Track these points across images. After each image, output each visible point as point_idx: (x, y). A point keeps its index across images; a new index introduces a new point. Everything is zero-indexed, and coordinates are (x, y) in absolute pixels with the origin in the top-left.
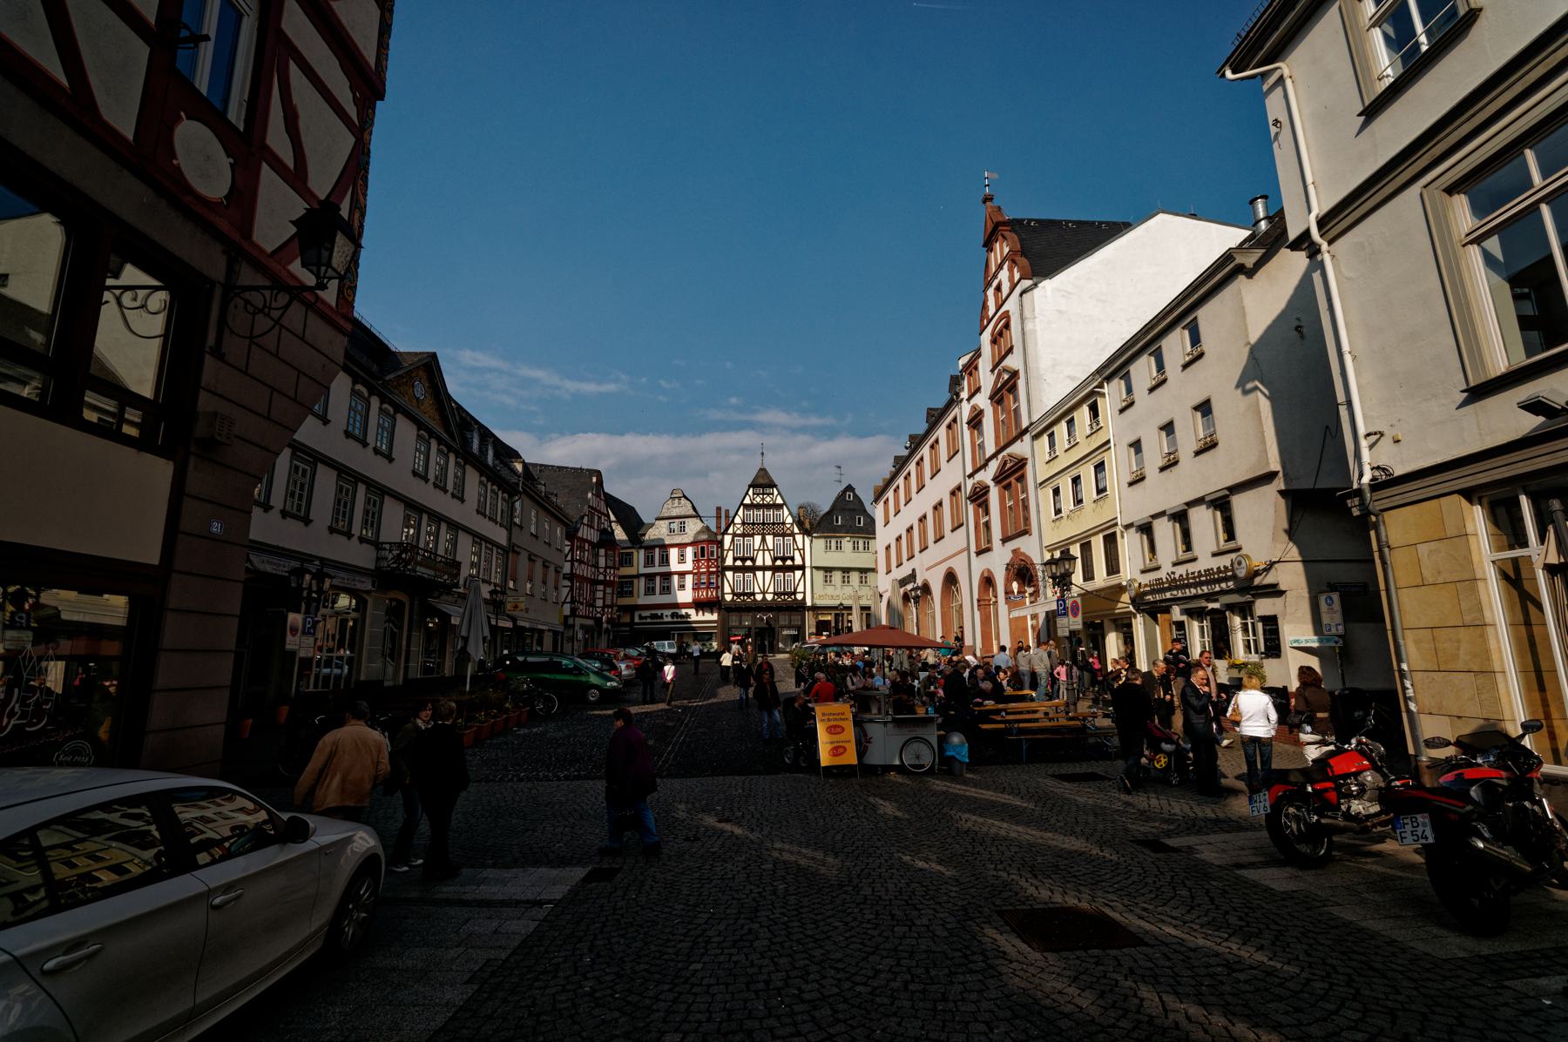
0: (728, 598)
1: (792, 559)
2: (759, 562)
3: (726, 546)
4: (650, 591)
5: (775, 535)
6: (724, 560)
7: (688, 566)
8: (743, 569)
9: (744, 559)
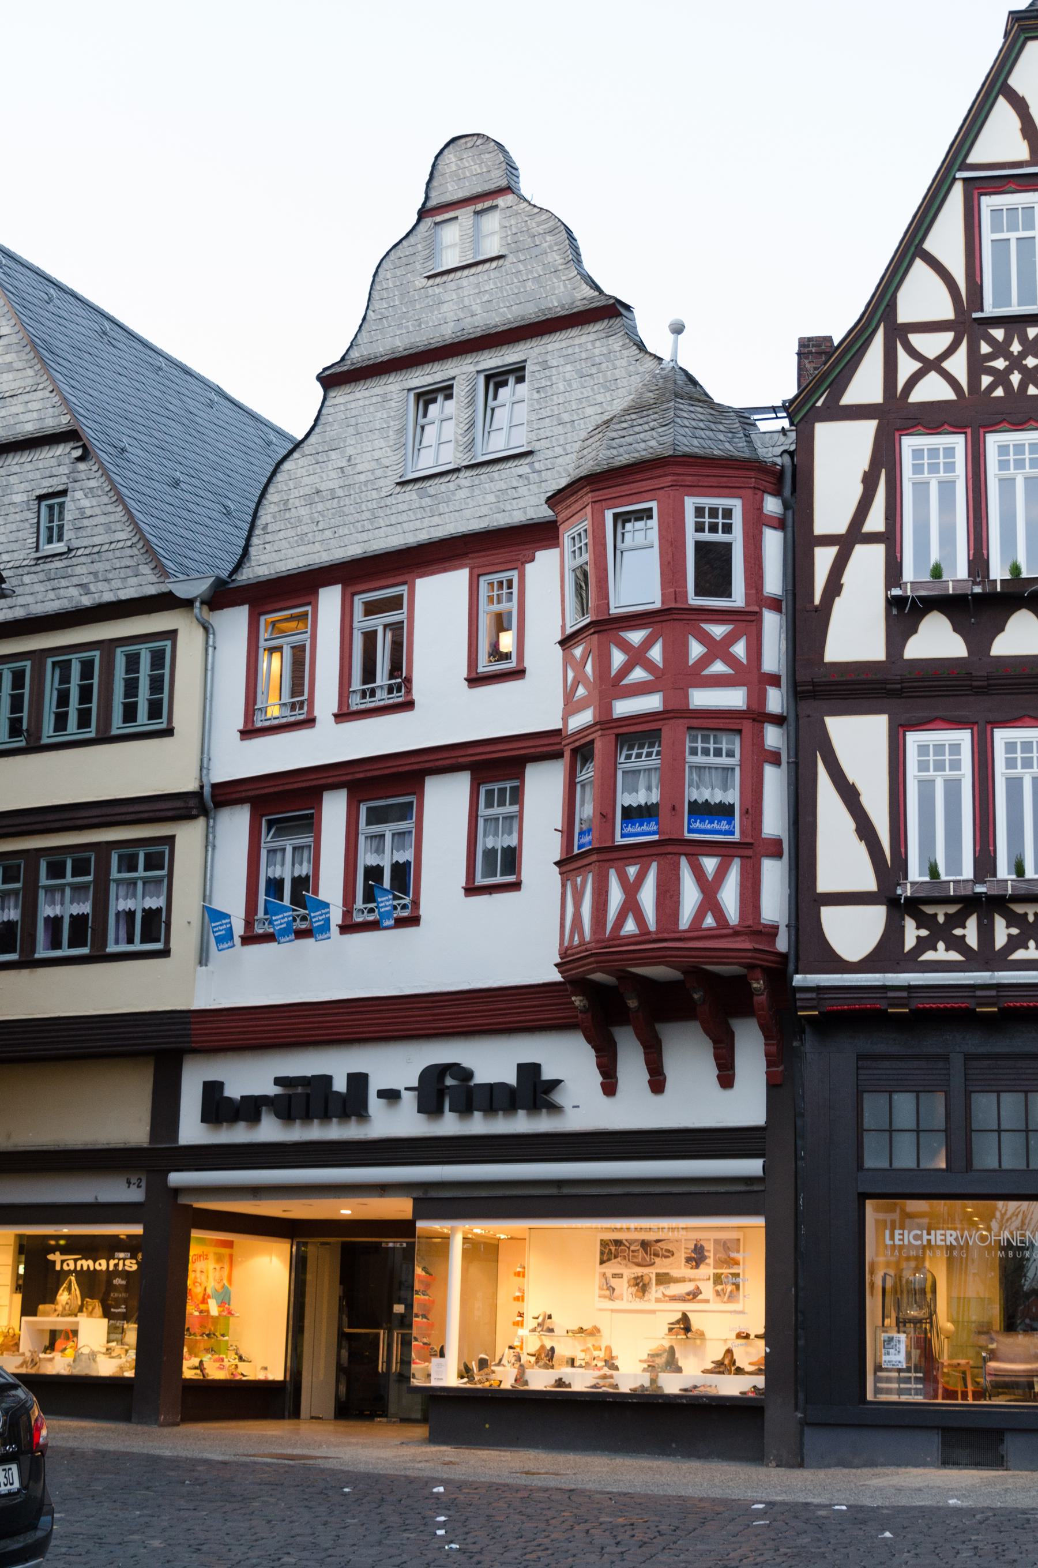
3: (832, 508)
4: (284, 909)
6: (808, 620)
7: (535, 703)
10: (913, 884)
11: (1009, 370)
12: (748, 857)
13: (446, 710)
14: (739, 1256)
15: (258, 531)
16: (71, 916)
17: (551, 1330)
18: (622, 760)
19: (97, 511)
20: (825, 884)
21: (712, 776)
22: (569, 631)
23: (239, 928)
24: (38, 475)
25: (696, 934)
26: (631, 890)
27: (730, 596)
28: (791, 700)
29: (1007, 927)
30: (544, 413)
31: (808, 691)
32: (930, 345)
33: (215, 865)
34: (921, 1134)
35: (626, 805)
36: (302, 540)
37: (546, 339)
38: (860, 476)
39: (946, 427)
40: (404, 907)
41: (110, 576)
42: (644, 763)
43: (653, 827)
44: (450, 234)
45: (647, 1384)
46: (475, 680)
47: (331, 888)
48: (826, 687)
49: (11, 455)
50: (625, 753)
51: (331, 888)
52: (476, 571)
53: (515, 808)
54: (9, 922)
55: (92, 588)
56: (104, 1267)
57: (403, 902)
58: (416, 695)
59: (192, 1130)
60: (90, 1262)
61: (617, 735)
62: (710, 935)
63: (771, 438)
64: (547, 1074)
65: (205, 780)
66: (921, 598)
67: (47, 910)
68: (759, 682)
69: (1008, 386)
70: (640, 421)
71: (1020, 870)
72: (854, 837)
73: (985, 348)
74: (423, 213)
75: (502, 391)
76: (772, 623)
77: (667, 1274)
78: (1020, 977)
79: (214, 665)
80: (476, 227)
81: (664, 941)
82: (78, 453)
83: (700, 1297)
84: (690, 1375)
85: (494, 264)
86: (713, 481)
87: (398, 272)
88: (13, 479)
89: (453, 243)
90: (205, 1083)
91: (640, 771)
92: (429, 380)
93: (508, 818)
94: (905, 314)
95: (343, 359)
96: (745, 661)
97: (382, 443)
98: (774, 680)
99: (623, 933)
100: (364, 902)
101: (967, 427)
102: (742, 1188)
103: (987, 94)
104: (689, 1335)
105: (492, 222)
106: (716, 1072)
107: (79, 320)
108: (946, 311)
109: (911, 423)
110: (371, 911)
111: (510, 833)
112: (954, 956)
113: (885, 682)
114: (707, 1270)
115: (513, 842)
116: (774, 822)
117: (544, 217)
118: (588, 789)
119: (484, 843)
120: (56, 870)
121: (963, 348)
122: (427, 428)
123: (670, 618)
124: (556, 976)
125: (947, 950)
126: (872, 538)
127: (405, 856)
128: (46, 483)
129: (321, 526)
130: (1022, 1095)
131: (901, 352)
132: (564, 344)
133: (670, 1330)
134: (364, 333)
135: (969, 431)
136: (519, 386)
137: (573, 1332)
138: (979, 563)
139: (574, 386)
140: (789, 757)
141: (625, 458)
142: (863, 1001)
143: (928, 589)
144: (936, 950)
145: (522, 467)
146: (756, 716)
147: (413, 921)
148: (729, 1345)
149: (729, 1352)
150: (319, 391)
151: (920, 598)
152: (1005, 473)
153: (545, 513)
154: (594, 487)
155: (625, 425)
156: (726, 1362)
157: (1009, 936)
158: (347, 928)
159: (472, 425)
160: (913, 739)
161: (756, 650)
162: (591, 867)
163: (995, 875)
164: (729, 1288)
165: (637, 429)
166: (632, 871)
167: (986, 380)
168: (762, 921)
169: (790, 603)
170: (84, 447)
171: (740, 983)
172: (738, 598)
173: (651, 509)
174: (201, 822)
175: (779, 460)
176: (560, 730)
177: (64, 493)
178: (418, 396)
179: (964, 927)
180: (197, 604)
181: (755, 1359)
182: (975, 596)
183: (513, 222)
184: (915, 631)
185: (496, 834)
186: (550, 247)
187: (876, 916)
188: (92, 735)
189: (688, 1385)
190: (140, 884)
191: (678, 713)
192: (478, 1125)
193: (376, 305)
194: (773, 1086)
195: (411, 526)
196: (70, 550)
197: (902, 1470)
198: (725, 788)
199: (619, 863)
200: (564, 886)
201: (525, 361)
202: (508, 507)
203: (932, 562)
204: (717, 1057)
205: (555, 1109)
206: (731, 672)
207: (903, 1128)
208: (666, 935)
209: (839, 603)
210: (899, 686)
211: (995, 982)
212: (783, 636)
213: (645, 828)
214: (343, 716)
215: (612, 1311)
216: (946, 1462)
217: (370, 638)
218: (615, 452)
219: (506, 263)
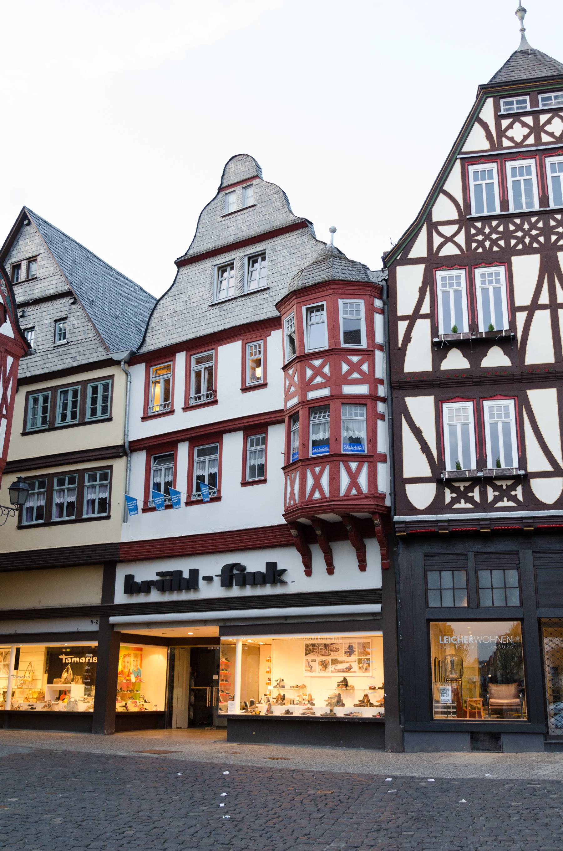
0: (421, 496)
3: (405, 304)
4: (161, 496)
6: (395, 353)
8: (475, 386)
9: (474, 346)
10: (449, 472)
11: (484, 240)
13: (234, 403)
15: (149, 331)
16: (68, 502)
17: (283, 687)
18: (312, 419)
19: (80, 325)
20: (407, 474)
22: (286, 363)
23: (141, 505)
24: (55, 311)
25: (348, 498)
28: (389, 391)
29: (493, 492)
30: (274, 271)
31: (397, 386)
32: (448, 231)
33: (131, 477)
34: (455, 590)
36: (168, 333)
37: (274, 239)
39: (456, 266)
40: (214, 493)
41: (85, 353)
42: (322, 420)
43: (327, 449)
44: (232, 198)
45: (328, 712)
46: (245, 389)
47: (181, 486)
48: (406, 385)
49: (44, 304)
50: (313, 416)
51: (181, 486)
52: (245, 341)
53: (264, 446)
54: (40, 506)
55: (78, 358)
56: (84, 661)
57: (213, 491)
58: (219, 398)
59: (120, 597)
60: (78, 659)
61: (310, 408)
62: (354, 498)
64: (280, 567)
65: (126, 440)
67: (57, 500)
68: (375, 382)
69: (484, 247)
70: (317, 267)
71: (498, 465)
73: (473, 231)
74: (220, 189)
75: (255, 265)
76: (379, 356)
77: (336, 659)
78: (500, 515)
79: (130, 390)
80: (243, 194)
82: (72, 301)
83: (352, 670)
84: (348, 708)
85: (251, 209)
86: (351, 292)
87: (210, 216)
88: (44, 314)
89: (233, 201)
90: (126, 576)
92: (224, 260)
93: (261, 451)
94: (436, 218)
95: (186, 254)
96: (367, 373)
97: (203, 289)
98: (381, 382)
99: (313, 498)
100: (197, 491)
101: (466, 266)
102: (371, 618)
103: (470, 121)
104: (347, 688)
105: (250, 192)
106: (358, 564)
107: (76, 251)
108: (455, 216)
109: (440, 265)
110: (199, 495)
111: (262, 458)
112: (469, 506)
113: (432, 380)
115: (263, 462)
116: (383, 446)
117: (273, 187)
118: (296, 434)
119: (250, 463)
120: (61, 482)
121: (463, 231)
122: (223, 282)
123: (333, 353)
124: (283, 521)
125: (465, 503)
126: (424, 316)
127: (214, 470)
128: (58, 314)
129: (177, 327)
130: (502, 571)
131: (435, 235)
132: (282, 241)
133: (338, 685)
134: (195, 242)
135: (467, 268)
136: (263, 262)
137: (294, 687)
138: (474, 325)
139: (287, 259)
140: (389, 416)
141: (310, 282)
142: (427, 528)
143: (451, 337)
144: (460, 503)
145: (265, 295)
146: (373, 398)
147: (218, 499)
148: (366, 692)
149: (366, 696)
150: (175, 268)
152: (484, 286)
153: (276, 313)
155: (310, 269)
156: (365, 701)
157: (494, 496)
158: (188, 504)
159: (242, 278)
161: (372, 368)
162: (298, 469)
163: (486, 467)
164: (365, 665)
165: (316, 271)
166: (317, 469)
167: (474, 245)
168: (379, 492)
169: (387, 346)
170: (75, 298)
171: (369, 521)
172: (364, 344)
173: (323, 305)
174: (124, 458)
176: (283, 410)
177: (66, 318)
178: (219, 268)
179: (473, 492)
180: (123, 363)
181: (379, 699)
182: (472, 339)
183: (259, 190)
184: (445, 357)
185: (255, 459)
186: (276, 200)
187: (432, 488)
188: (77, 422)
189: (348, 712)
190: (97, 487)
192: (249, 592)
193: (200, 230)
194: (385, 570)
195: (216, 324)
196: (68, 343)
197: (453, 754)
198: (360, 432)
199: (311, 466)
200: (286, 479)
201: (265, 249)
202: (259, 313)
204: (358, 557)
205: (283, 583)
206: (361, 377)
207: (446, 586)
208: (334, 499)
209: (410, 346)
210: (439, 382)
212: (385, 362)
213: (323, 450)
214: (187, 408)
215: (311, 677)
216: (473, 749)
217: (198, 375)
218: (306, 281)
219: (256, 208)
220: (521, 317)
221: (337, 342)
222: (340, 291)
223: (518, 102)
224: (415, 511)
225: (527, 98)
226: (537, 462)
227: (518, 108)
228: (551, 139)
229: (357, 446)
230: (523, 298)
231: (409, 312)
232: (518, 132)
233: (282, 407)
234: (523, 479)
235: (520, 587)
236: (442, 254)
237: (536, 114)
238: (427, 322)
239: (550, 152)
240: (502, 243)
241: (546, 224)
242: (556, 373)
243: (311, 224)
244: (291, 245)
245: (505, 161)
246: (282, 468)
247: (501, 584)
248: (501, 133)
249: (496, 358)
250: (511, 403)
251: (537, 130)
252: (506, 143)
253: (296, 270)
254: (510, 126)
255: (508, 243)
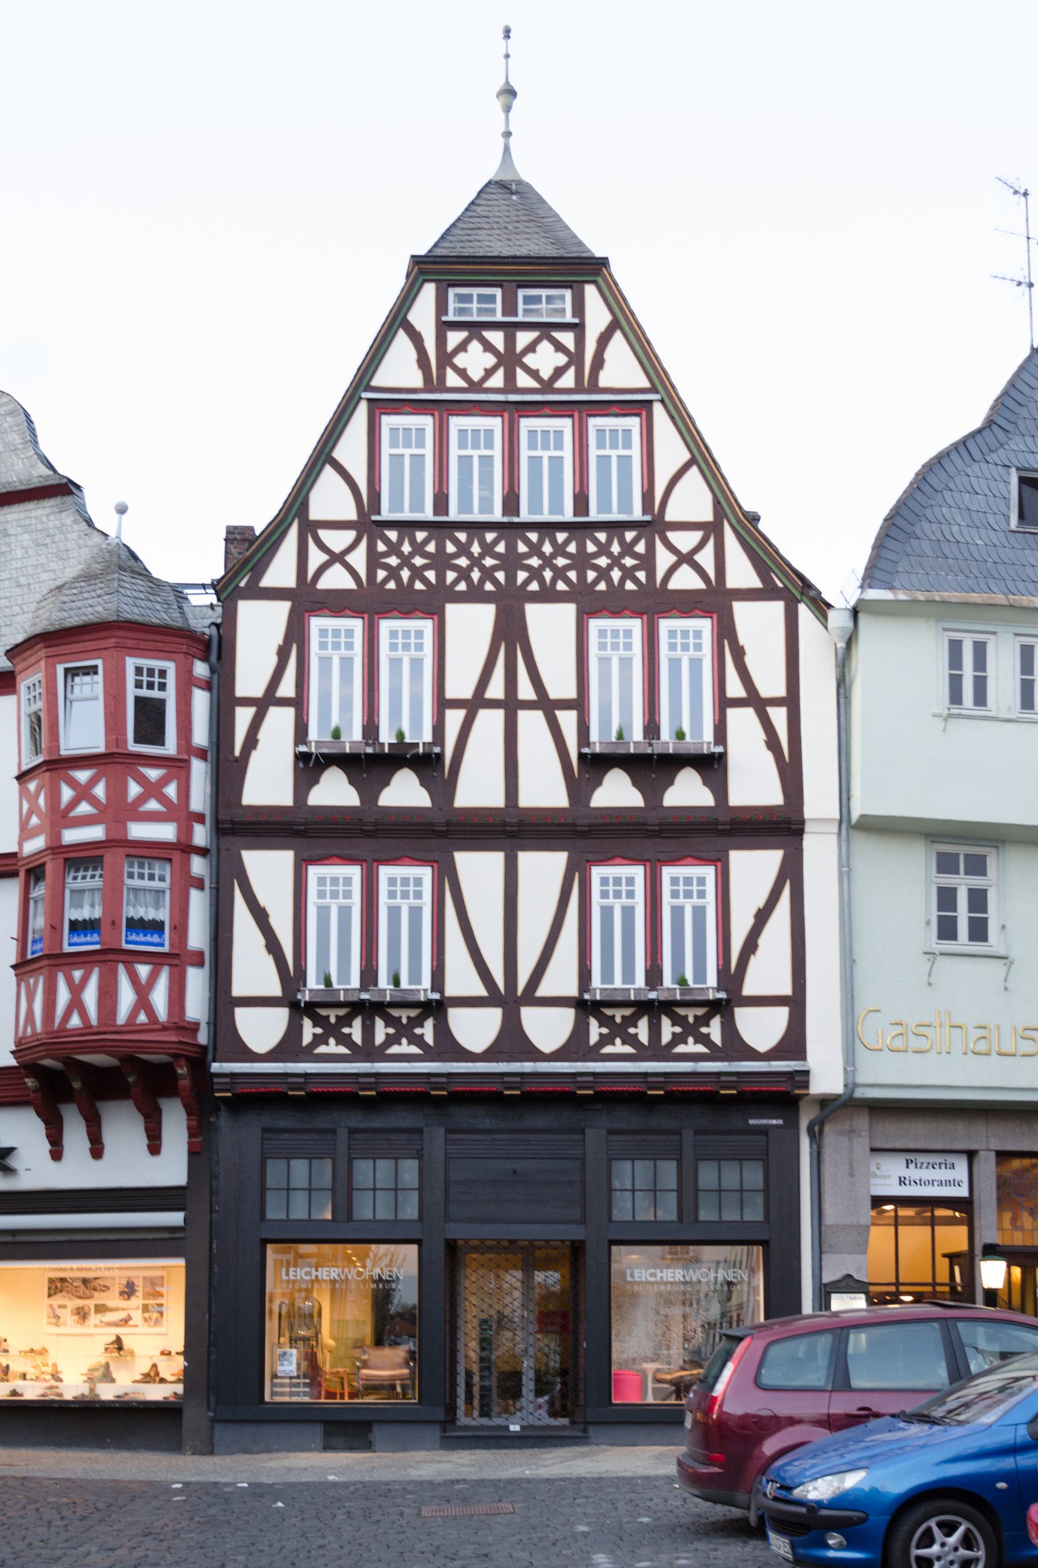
0: (261, 1029)
1: (711, 766)
2: (478, 788)
3: (251, 677)
5: (591, 604)
6: (229, 769)
8: (367, 838)
9: (370, 766)
10: (311, 991)
12: (177, 966)
14: (163, 1290)
17: (6, 1351)
20: (238, 990)
21: (147, 895)
22: (25, 768)
26: (76, 990)
27: (163, 744)
35: (73, 919)
38: (275, 649)
42: (89, 883)
43: (96, 938)
45: (86, 1392)
48: (244, 826)
61: (66, 859)
62: (142, 1030)
63: (201, 611)
66: (323, 755)
68: (187, 819)
71: (396, 981)
72: (264, 951)
73: (381, 547)
76: (199, 770)
77: (104, 1305)
81: (103, 1033)
83: (131, 1323)
84: (123, 1385)
91: (84, 891)
96: (175, 801)
98: (200, 818)
101: (364, 612)
102: (167, 1235)
104: (122, 1353)
113: (292, 823)
114: (137, 1301)
116: (198, 937)
126: (284, 702)
130: (393, 1162)
133: (106, 1349)
135: (366, 616)
137: (25, 1352)
138: (371, 729)
146: (185, 848)
148: (155, 1360)
149: (155, 1366)
151: (322, 755)
152: (394, 654)
154: (47, 643)
155: (75, 591)
156: (152, 1374)
160: (314, 872)
161: (184, 792)
162: (42, 971)
163: (376, 985)
164: (155, 1315)
166: (77, 974)
167: (381, 574)
168: (187, 1019)
171: (167, 1069)
172: (170, 747)
175: (207, 631)
181: (176, 1371)
182: (367, 755)
187: (281, 1016)
189: (120, 1392)
191: (117, 842)
197: (292, 1455)
198: (157, 907)
199: (66, 968)
200: (19, 986)
203: (333, 725)
207: (298, 1185)
209: (254, 754)
210: (303, 828)
211: (374, 1071)
212: (208, 781)
213: (89, 939)
215: (58, 1335)
216: (327, 1447)
220: (454, 719)
221: (121, 741)
222: (130, 643)
223: (482, 298)
224: (248, 1055)
225: (498, 292)
226: (462, 980)
227: (480, 311)
228: (533, 384)
229: (152, 935)
230: (461, 684)
231: (258, 692)
232: (475, 360)
233: (13, 848)
234: (436, 1009)
235: (420, 1189)
236: (323, 584)
237: (510, 329)
238: (288, 714)
239: (529, 408)
240: (431, 575)
241: (511, 547)
242: (505, 825)
243: (78, 487)
244: (39, 527)
245: (449, 415)
246: (13, 967)
247: (390, 1184)
248: (446, 358)
249: (405, 792)
250: (426, 873)
251: (510, 360)
252: (453, 380)
253: (48, 581)
254: (462, 347)
255: (441, 577)
